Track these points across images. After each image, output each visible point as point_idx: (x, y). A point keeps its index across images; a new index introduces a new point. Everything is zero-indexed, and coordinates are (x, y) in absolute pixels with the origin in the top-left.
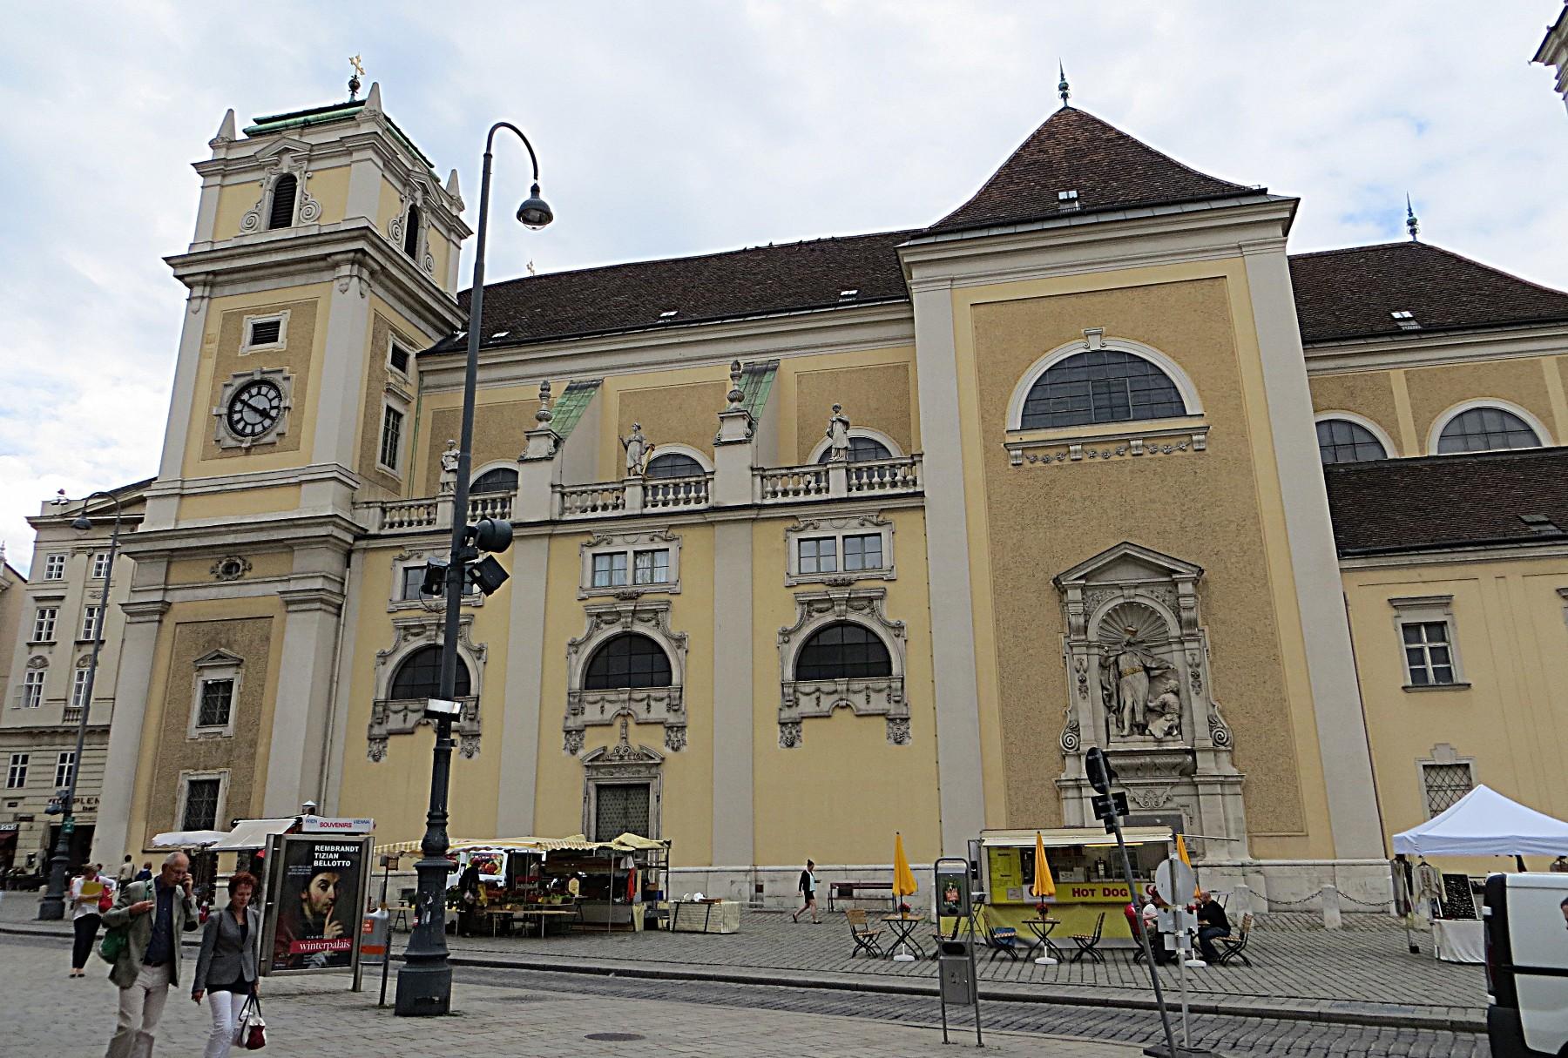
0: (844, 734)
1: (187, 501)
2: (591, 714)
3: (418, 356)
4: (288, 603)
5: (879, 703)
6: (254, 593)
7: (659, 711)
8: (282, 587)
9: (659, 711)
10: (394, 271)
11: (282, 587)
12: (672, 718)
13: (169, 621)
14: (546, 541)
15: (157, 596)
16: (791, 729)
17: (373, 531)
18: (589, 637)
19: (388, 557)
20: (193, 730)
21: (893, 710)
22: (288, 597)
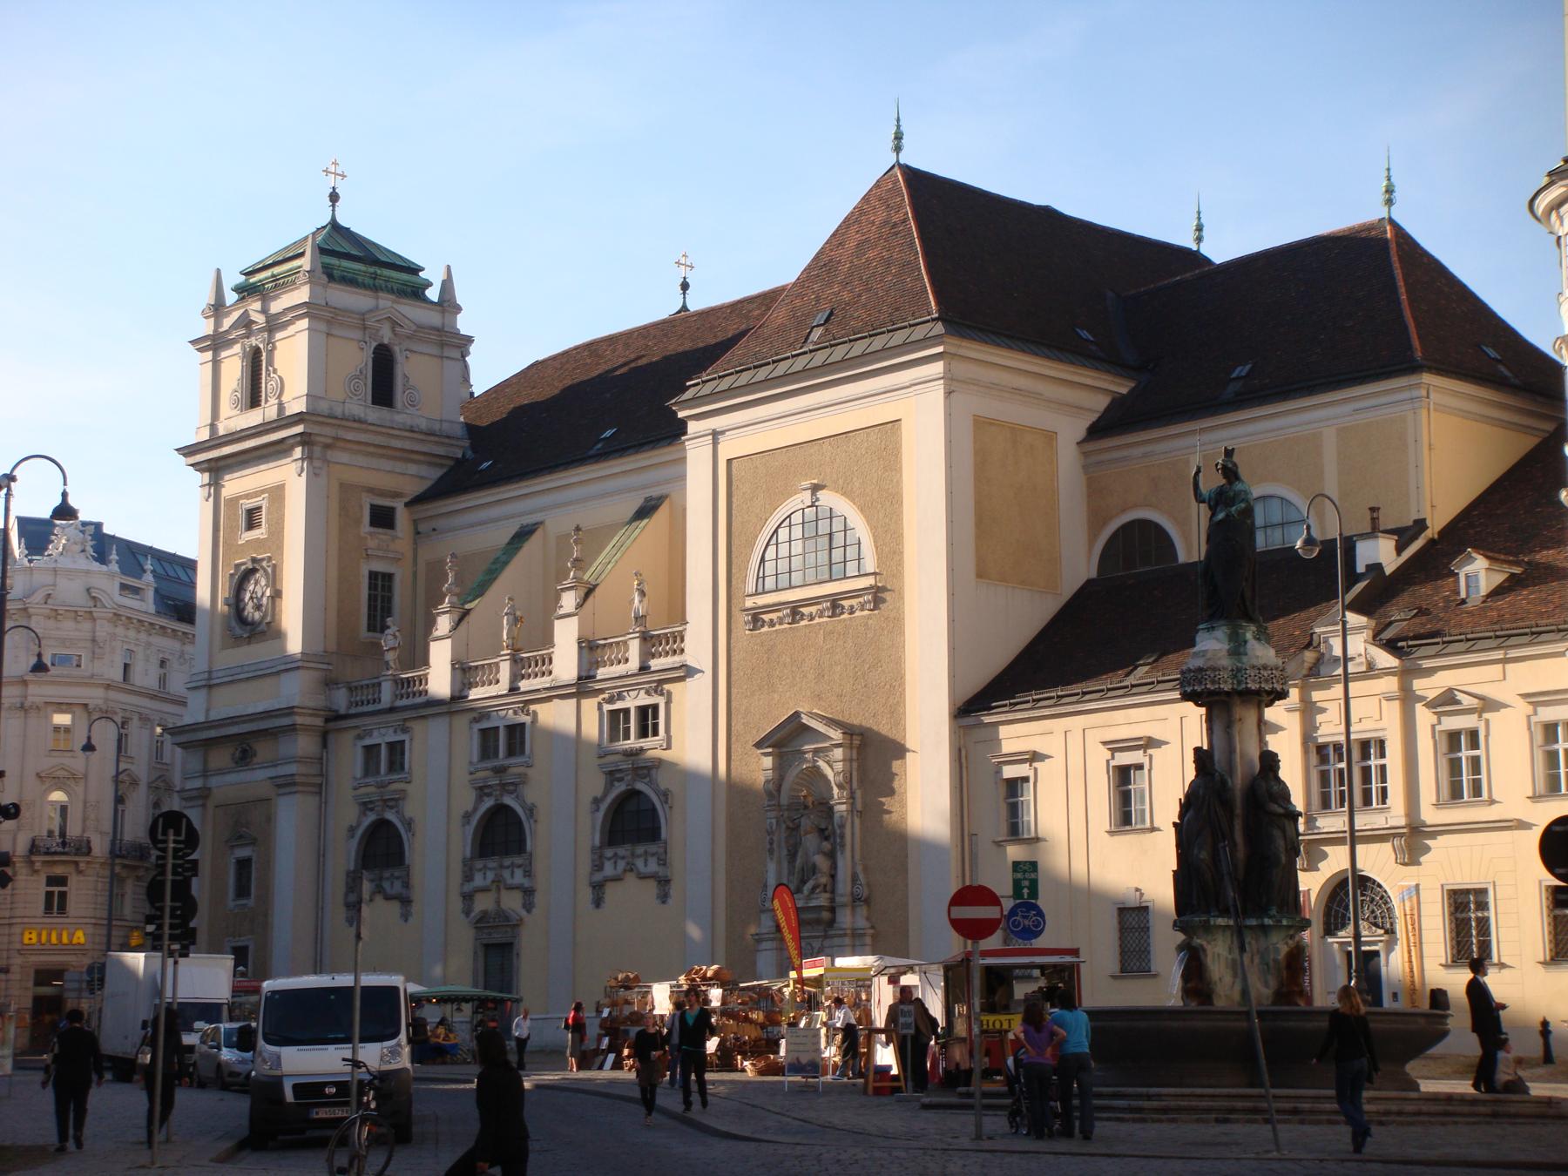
0: (631, 896)
1: (217, 693)
2: (478, 881)
3: (407, 505)
4: (279, 786)
5: (653, 866)
6: (255, 779)
7: (519, 878)
8: (272, 772)
9: (519, 878)
10: (350, 436)
11: (272, 772)
12: (526, 882)
13: (210, 804)
14: (446, 719)
15: (198, 783)
16: (598, 888)
17: (343, 711)
18: (475, 809)
19: (350, 735)
20: (231, 904)
21: (661, 871)
22: (280, 781)
